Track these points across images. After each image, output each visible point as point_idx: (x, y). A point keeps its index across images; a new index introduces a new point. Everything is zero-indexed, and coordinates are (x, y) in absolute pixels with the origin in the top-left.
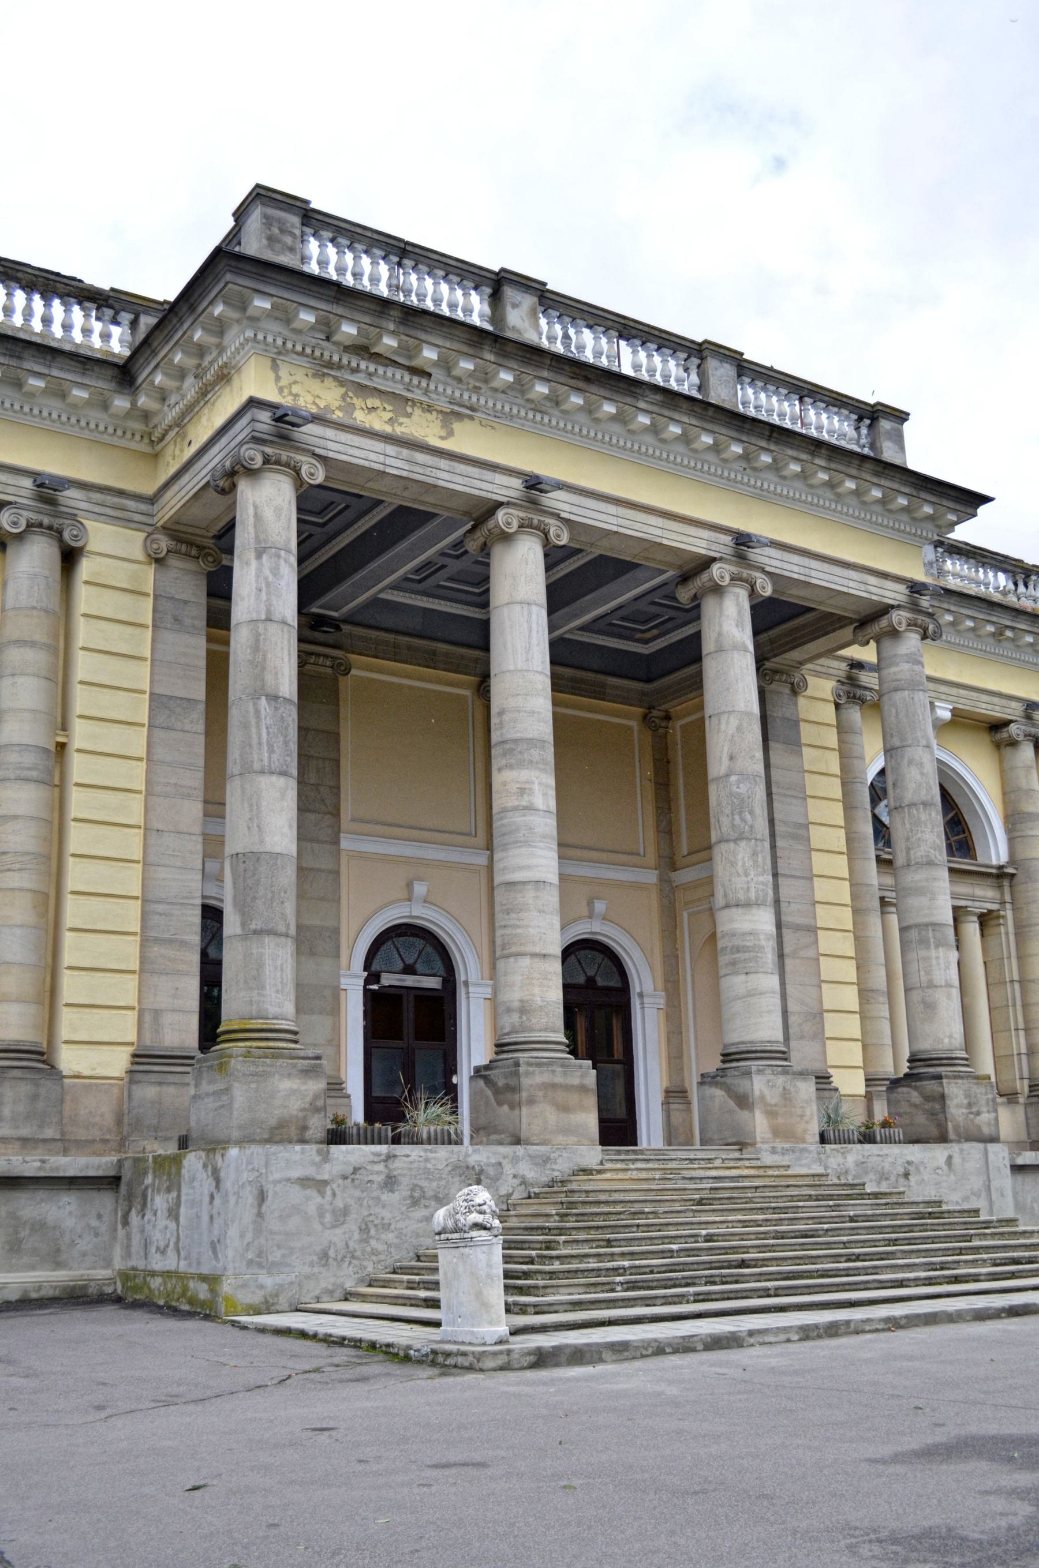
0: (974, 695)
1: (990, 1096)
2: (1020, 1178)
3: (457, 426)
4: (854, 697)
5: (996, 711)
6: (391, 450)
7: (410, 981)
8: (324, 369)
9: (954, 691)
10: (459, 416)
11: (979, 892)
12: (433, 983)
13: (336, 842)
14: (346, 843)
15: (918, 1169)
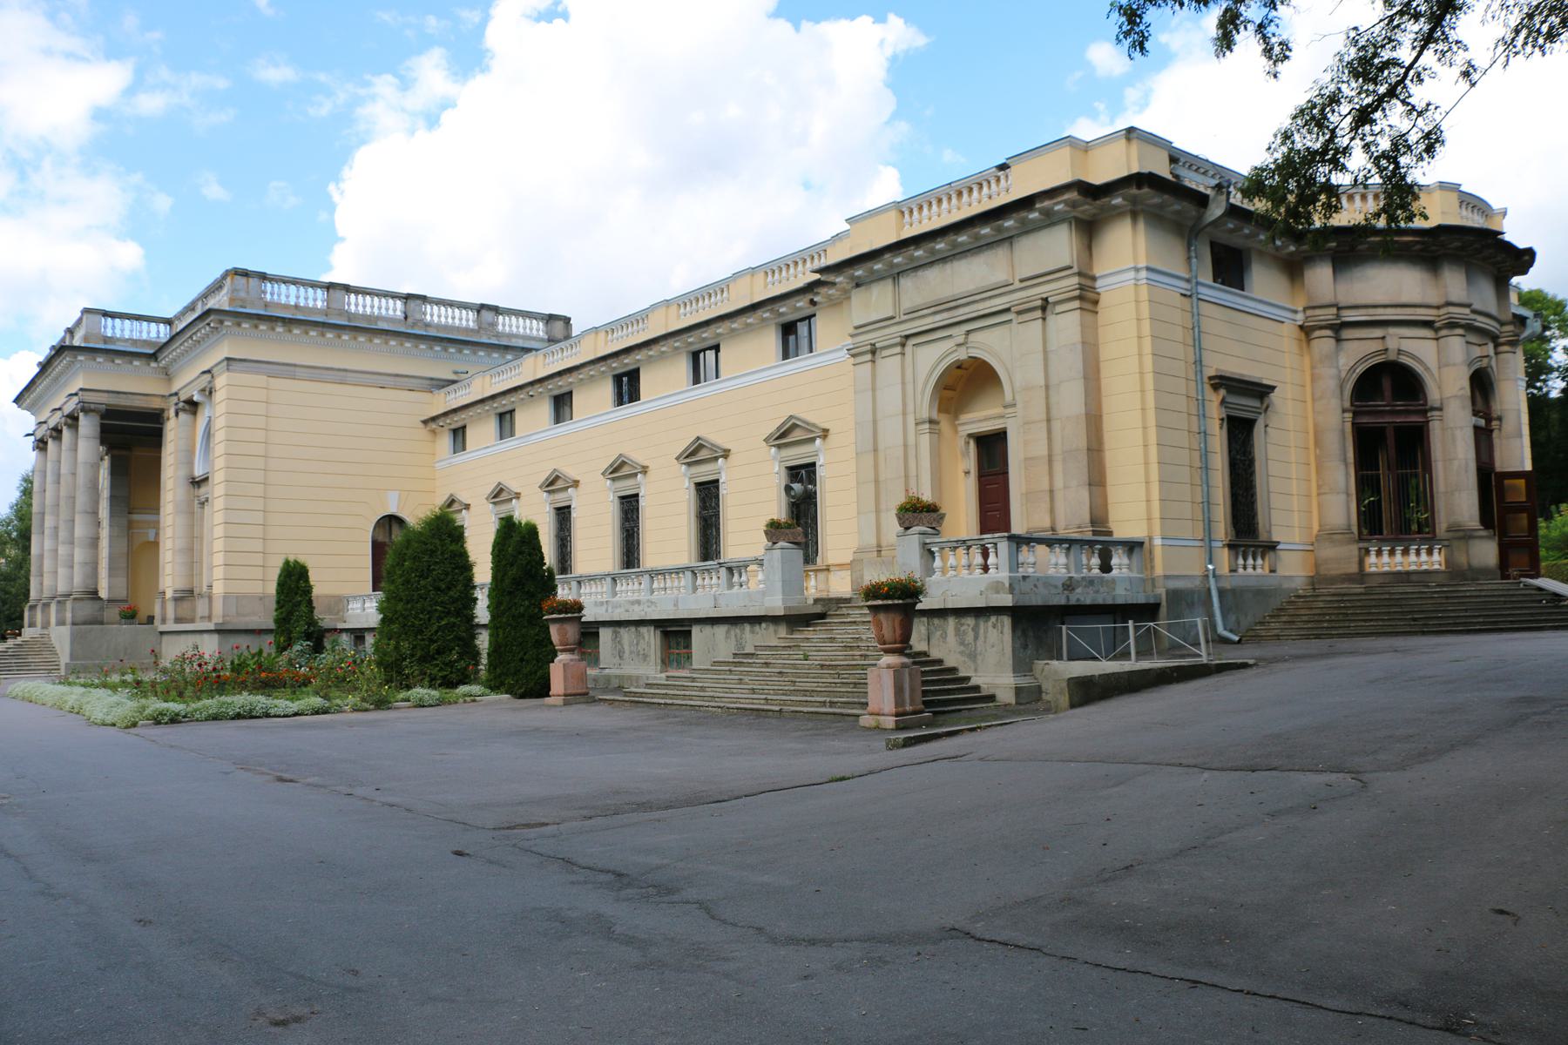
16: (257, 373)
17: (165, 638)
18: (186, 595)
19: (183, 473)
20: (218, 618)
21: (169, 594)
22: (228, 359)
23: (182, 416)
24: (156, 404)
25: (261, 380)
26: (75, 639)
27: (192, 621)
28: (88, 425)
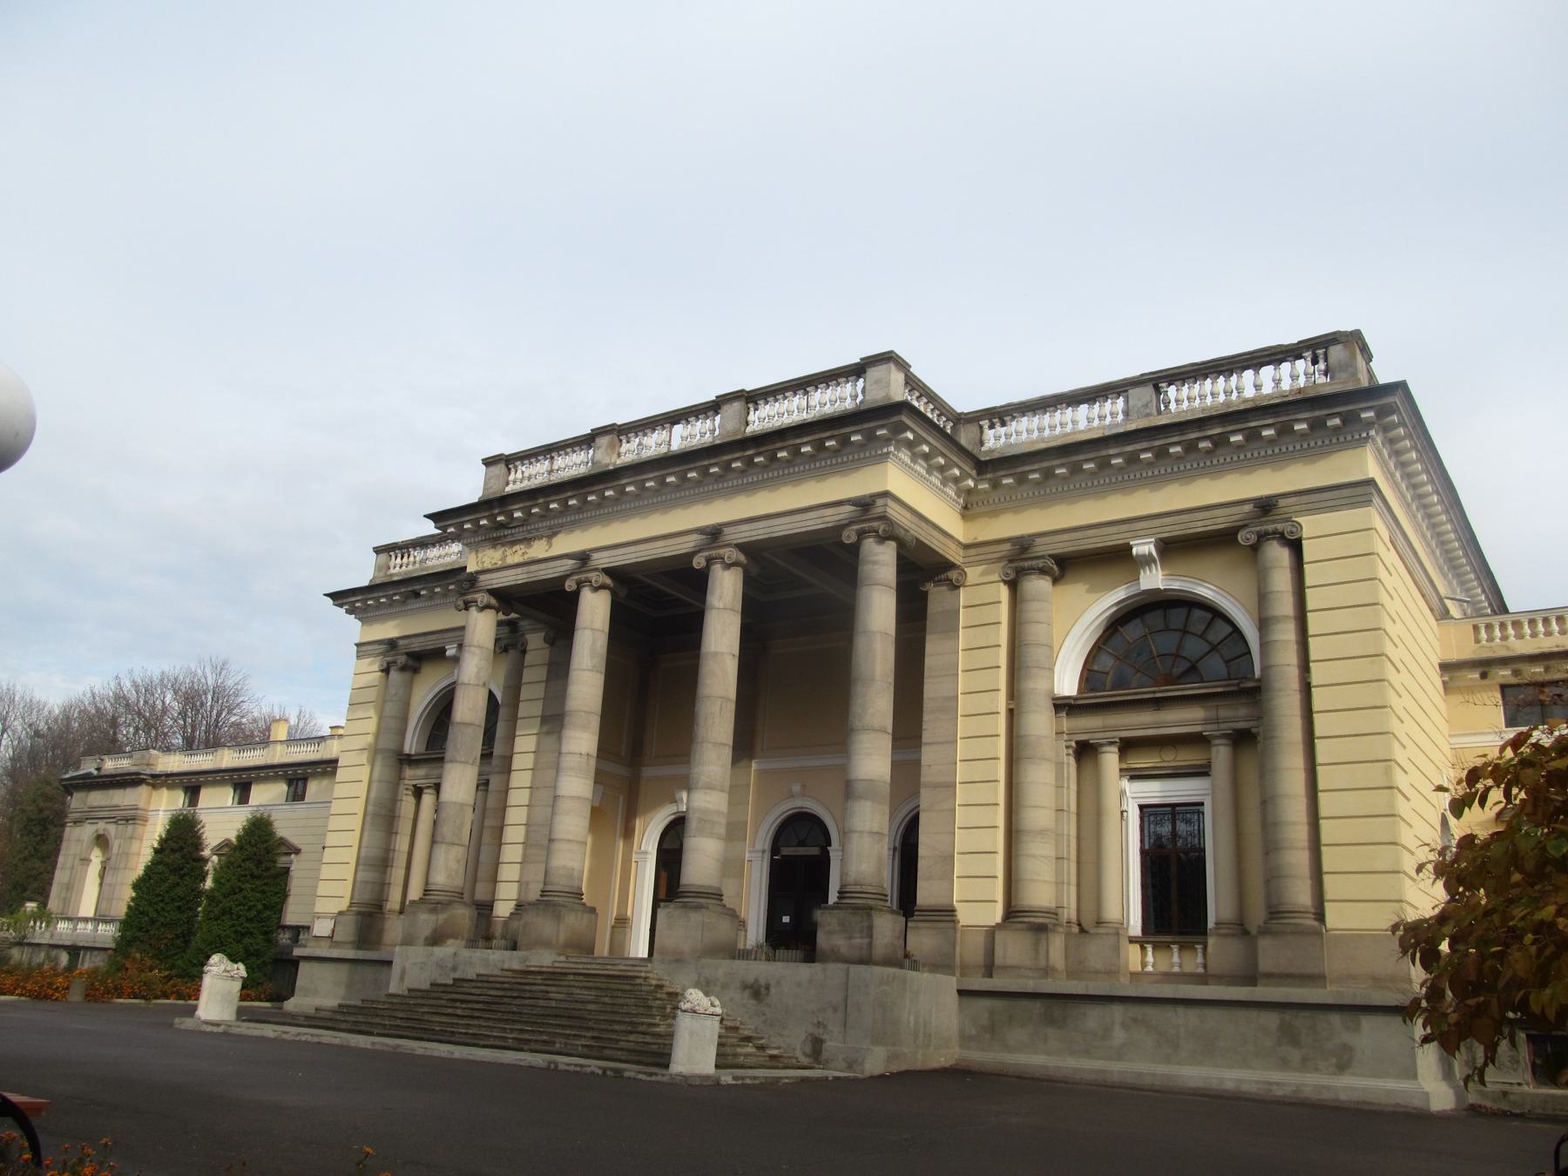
0: (1185, 517)
1: (866, 924)
2: (966, 1000)
3: (556, 540)
4: (1023, 569)
5: (1220, 521)
6: (519, 570)
7: (802, 851)
8: (495, 542)
9: (1157, 522)
10: (555, 534)
11: (1224, 713)
12: (815, 851)
15: (778, 983)
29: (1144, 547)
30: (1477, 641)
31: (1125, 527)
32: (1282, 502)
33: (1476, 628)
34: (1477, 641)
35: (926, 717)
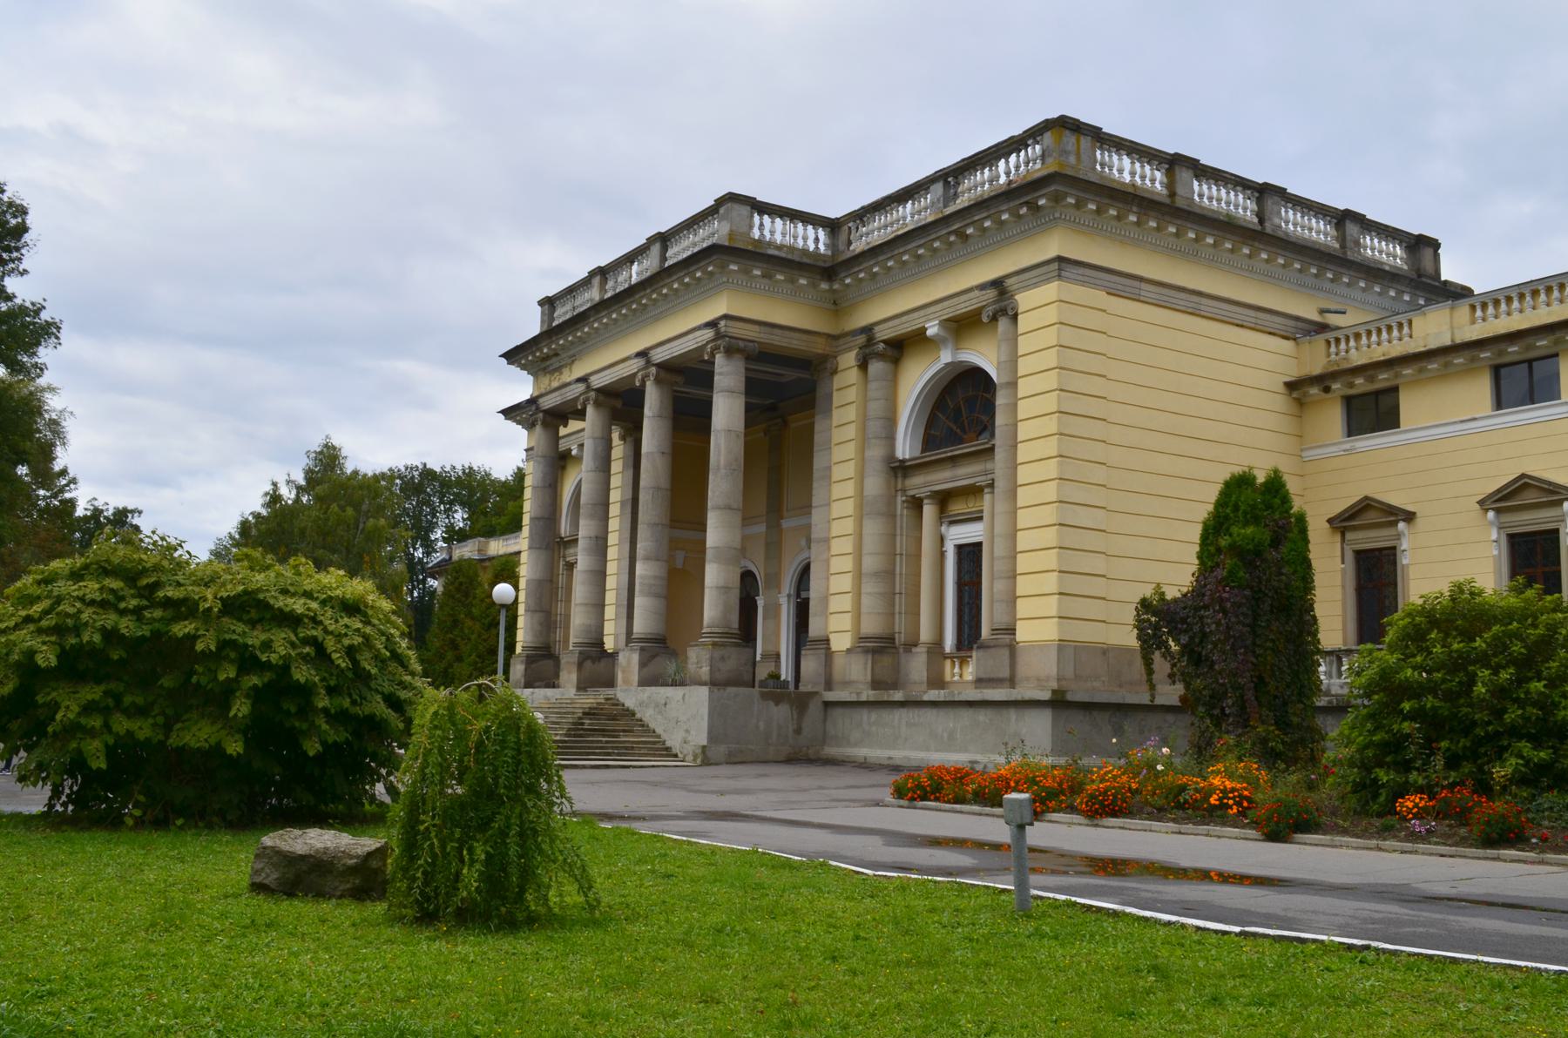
3: (575, 367)
13: (779, 525)
14: (785, 524)
16: (1096, 286)
17: (837, 713)
18: (883, 648)
19: (876, 452)
20: (1039, 674)
21: (841, 643)
22: (1060, 259)
23: (876, 367)
24: (819, 347)
25: (1099, 297)
26: (716, 712)
27: (895, 686)
28: (728, 377)
29: (933, 330)
30: (1329, 355)
31: (922, 313)
32: (1009, 282)
33: (1328, 343)
34: (1329, 355)
35: (815, 485)
